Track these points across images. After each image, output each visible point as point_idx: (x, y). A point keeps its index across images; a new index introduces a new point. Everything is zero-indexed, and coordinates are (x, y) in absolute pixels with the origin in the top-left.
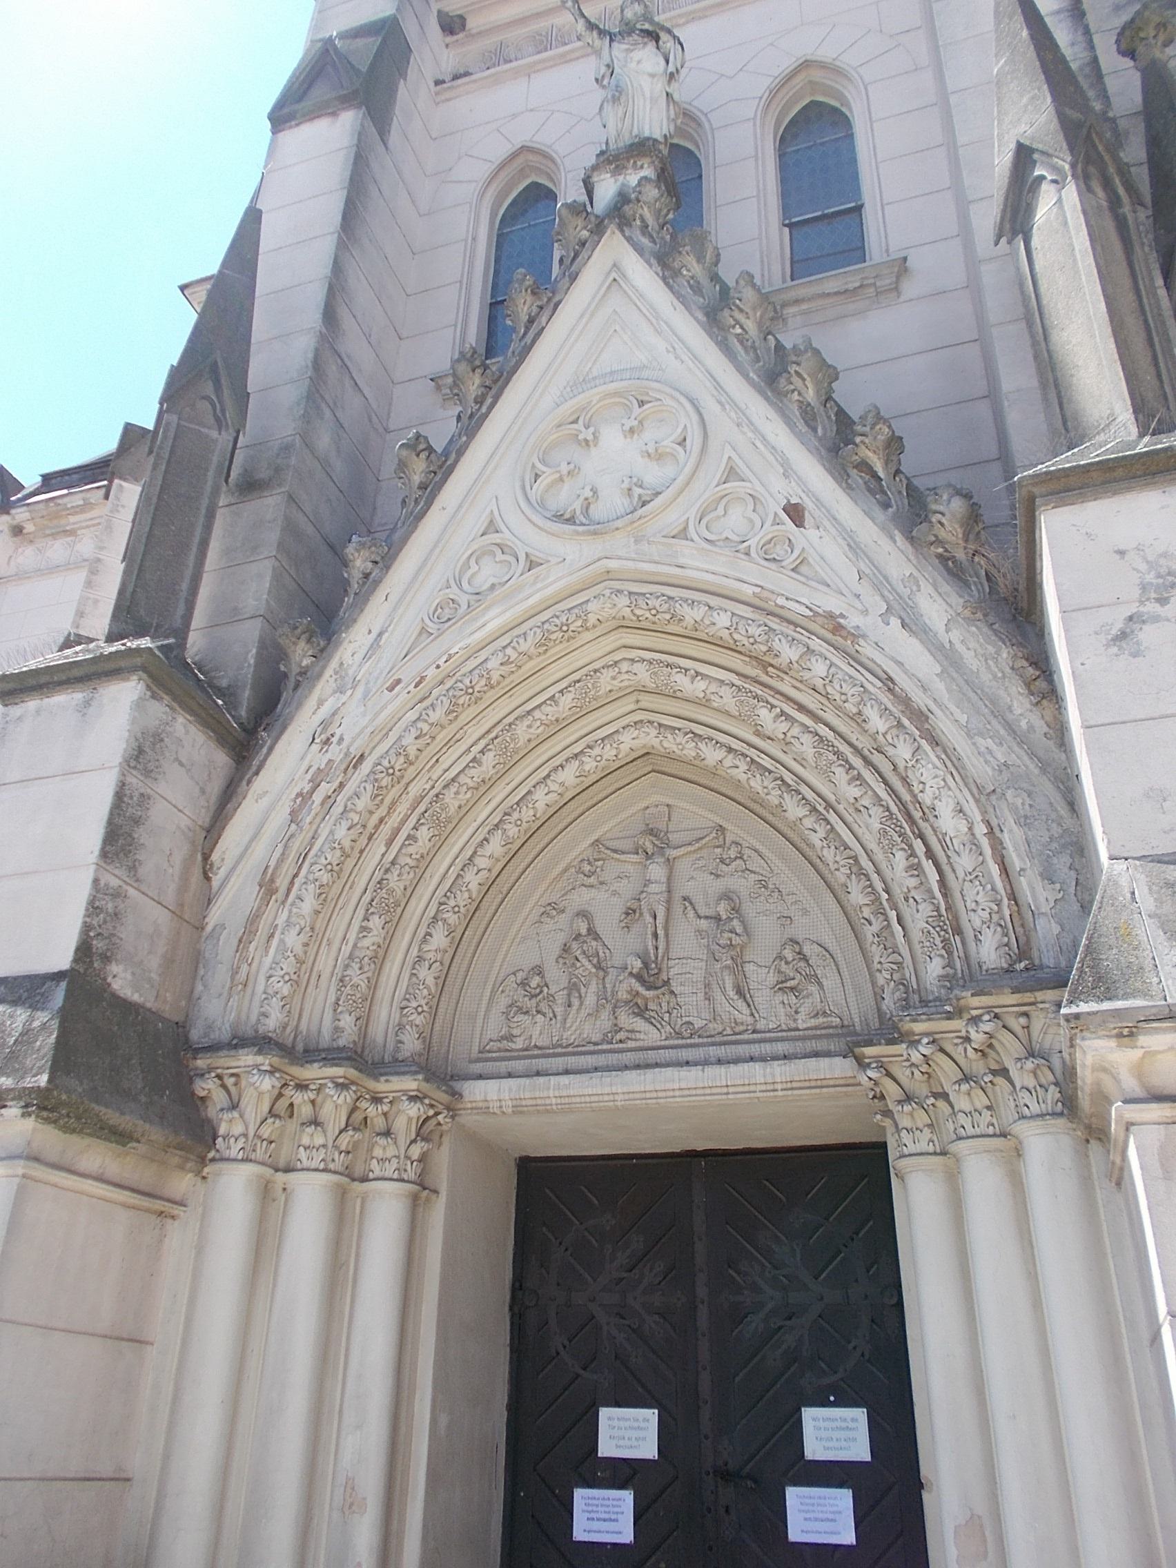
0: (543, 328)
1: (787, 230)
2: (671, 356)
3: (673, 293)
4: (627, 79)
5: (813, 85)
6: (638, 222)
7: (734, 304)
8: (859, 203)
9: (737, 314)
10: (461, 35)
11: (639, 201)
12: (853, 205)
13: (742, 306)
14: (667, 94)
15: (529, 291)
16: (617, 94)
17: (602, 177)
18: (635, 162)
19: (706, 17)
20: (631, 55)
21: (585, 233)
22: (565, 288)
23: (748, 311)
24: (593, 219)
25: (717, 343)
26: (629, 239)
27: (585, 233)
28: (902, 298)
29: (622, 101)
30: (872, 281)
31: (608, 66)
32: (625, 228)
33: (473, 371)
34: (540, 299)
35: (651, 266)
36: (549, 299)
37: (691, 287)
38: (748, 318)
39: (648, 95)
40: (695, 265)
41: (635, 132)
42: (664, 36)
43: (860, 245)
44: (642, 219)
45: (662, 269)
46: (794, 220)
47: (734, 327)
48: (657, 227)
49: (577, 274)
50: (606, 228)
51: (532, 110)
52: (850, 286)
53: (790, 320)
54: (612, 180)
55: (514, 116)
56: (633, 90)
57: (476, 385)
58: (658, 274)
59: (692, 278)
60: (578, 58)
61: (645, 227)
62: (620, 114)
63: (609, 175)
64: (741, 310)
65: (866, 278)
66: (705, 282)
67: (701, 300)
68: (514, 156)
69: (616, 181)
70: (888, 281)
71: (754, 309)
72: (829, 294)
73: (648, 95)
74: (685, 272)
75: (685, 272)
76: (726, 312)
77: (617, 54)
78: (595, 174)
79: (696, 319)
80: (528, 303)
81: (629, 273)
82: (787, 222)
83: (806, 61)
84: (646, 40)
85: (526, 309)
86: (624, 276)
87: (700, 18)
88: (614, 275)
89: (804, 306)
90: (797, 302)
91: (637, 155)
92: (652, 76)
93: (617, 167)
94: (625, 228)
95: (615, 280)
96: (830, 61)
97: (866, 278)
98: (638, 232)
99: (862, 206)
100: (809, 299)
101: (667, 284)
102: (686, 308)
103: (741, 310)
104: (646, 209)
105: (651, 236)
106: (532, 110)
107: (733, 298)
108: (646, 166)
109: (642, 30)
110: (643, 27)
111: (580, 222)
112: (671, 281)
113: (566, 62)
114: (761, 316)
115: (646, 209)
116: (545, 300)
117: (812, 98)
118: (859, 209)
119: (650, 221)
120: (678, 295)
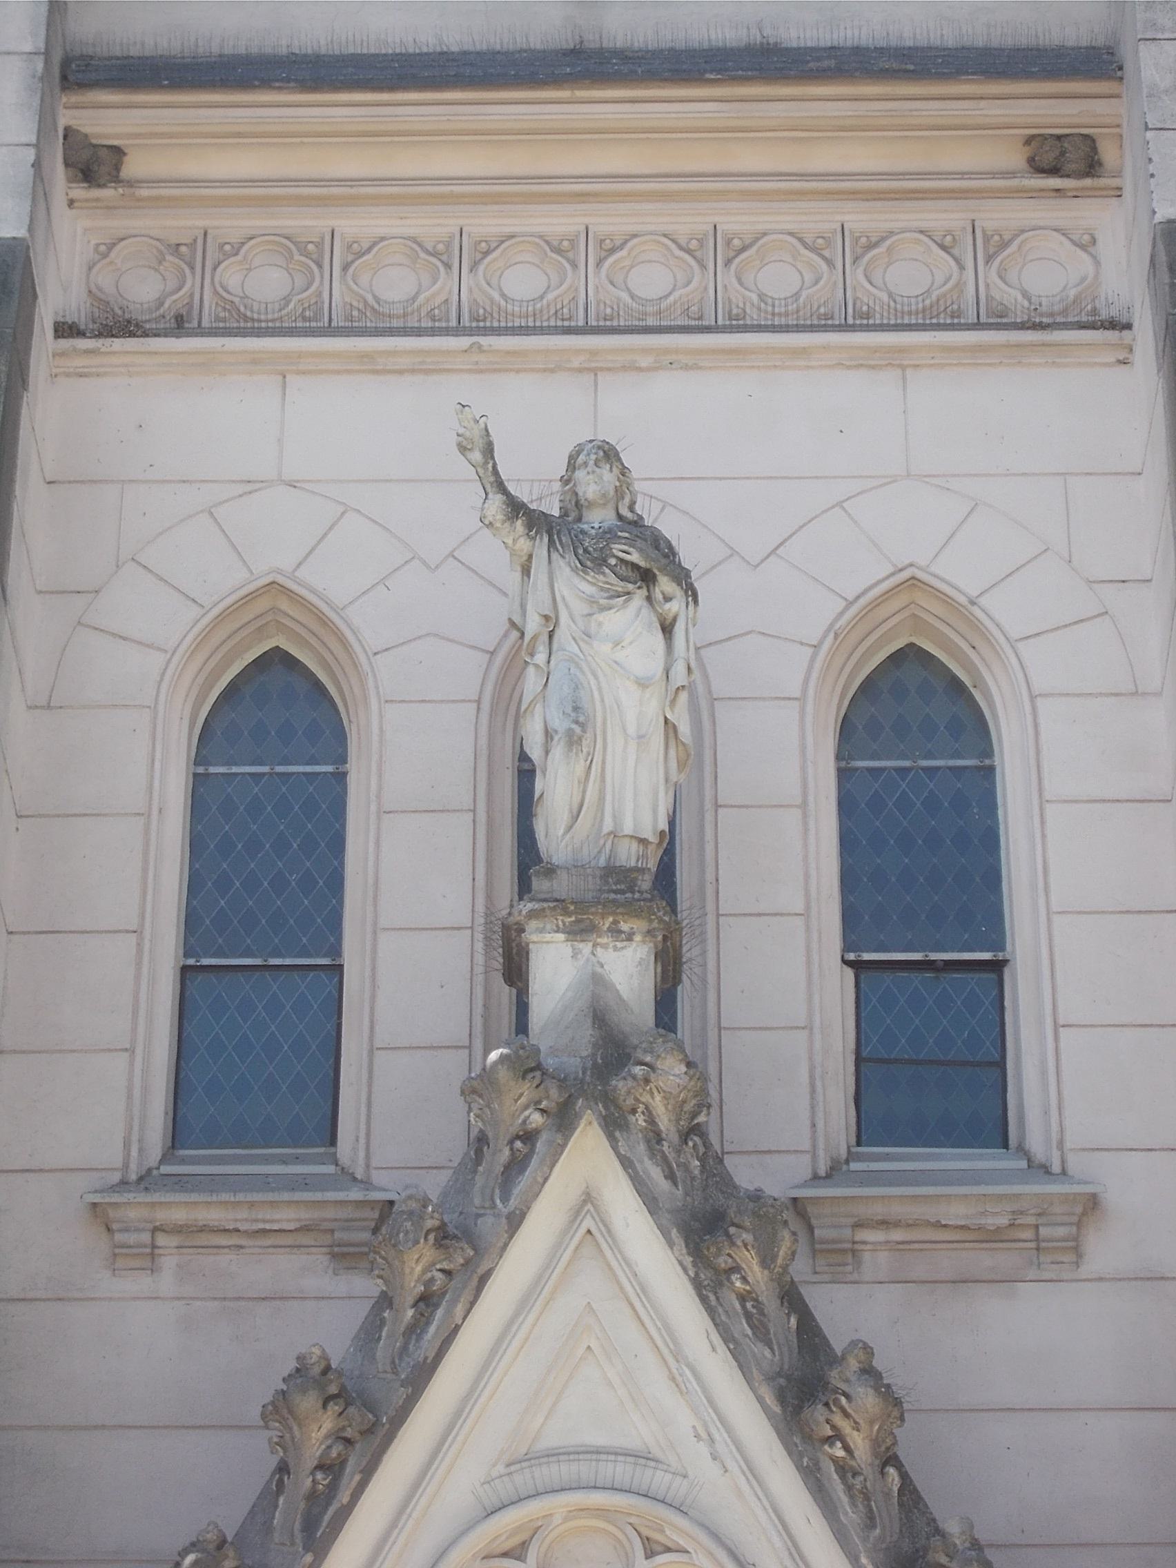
0: (457, 1328)
1: (850, 973)
2: (703, 1449)
3: (716, 1325)
4: (593, 682)
5: (917, 623)
6: (641, 1120)
7: (836, 1402)
8: (1000, 956)
9: (838, 1419)
10: (107, 193)
12: (986, 956)
13: (849, 1410)
14: (666, 720)
15: (431, 1237)
16: (578, 730)
17: (548, 937)
18: (615, 922)
19: (700, 368)
20: (601, 617)
22: (500, 1244)
23: (861, 1422)
24: (554, 1093)
25: (799, 1467)
26: (626, 1163)
27: (537, 1119)
28: (1086, 1270)
29: (584, 742)
30: (1031, 1220)
31: (547, 618)
32: (617, 1134)
33: (325, 1406)
34: (449, 1258)
35: (671, 1244)
36: (467, 1262)
37: (748, 1316)
38: (858, 1430)
39: (632, 730)
40: (756, 1268)
41: (608, 825)
42: (665, 584)
43: (997, 1057)
45: (695, 1264)
46: (866, 956)
47: (829, 1440)
48: (675, 1138)
49: (523, 1216)
50: (578, 1116)
51: (292, 485)
52: (991, 1222)
53: (867, 1257)
54: (567, 949)
55: (251, 485)
56: (604, 712)
57: (324, 1431)
58: (685, 1269)
60: (401, 372)
61: (654, 1137)
62: (580, 768)
63: (561, 937)
64: (846, 1415)
65: (1022, 1213)
67: (767, 1353)
69: (574, 956)
70: (1061, 1231)
73: (632, 730)
74: (738, 1284)
75: (738, 1284)
76: (820, 1413)
77: (566, 593)
78: (533, 925)
79: (760, 1400)
81: (618, 1224)
82: (851, 956)
83: (913, 578)
84: (630, 587)
85: (419, 1269)
86: (609, 1231)
87: (686, 368)
88: (588, 1223)
89: (897, 1235)
90: (885, 1224)
91: (622, 914)
92: (643, 684)
93: (578, 921)
94: (617, 1134)
95: (589, 1232)
96: (962, 600)
97: (1022, 1213)
98: (642, 1147)
99: (1005, 962)
100: (909, 1225)
101: (704, 1300)
102: (741, 1367)
103: (846, 1415)
104: (658, 1098)
106: (292, 485)
107: (836, 1390)
108: (638, 938)
110: (628, 557)
111: (527, 1090)
112: (712, 1297)
113: (377, 372)
114: (879, 1430)
115: (658, 1098)
117: (914, 640)
118: (997, 967)
119: (665, 1123)
120: (727, 1337)
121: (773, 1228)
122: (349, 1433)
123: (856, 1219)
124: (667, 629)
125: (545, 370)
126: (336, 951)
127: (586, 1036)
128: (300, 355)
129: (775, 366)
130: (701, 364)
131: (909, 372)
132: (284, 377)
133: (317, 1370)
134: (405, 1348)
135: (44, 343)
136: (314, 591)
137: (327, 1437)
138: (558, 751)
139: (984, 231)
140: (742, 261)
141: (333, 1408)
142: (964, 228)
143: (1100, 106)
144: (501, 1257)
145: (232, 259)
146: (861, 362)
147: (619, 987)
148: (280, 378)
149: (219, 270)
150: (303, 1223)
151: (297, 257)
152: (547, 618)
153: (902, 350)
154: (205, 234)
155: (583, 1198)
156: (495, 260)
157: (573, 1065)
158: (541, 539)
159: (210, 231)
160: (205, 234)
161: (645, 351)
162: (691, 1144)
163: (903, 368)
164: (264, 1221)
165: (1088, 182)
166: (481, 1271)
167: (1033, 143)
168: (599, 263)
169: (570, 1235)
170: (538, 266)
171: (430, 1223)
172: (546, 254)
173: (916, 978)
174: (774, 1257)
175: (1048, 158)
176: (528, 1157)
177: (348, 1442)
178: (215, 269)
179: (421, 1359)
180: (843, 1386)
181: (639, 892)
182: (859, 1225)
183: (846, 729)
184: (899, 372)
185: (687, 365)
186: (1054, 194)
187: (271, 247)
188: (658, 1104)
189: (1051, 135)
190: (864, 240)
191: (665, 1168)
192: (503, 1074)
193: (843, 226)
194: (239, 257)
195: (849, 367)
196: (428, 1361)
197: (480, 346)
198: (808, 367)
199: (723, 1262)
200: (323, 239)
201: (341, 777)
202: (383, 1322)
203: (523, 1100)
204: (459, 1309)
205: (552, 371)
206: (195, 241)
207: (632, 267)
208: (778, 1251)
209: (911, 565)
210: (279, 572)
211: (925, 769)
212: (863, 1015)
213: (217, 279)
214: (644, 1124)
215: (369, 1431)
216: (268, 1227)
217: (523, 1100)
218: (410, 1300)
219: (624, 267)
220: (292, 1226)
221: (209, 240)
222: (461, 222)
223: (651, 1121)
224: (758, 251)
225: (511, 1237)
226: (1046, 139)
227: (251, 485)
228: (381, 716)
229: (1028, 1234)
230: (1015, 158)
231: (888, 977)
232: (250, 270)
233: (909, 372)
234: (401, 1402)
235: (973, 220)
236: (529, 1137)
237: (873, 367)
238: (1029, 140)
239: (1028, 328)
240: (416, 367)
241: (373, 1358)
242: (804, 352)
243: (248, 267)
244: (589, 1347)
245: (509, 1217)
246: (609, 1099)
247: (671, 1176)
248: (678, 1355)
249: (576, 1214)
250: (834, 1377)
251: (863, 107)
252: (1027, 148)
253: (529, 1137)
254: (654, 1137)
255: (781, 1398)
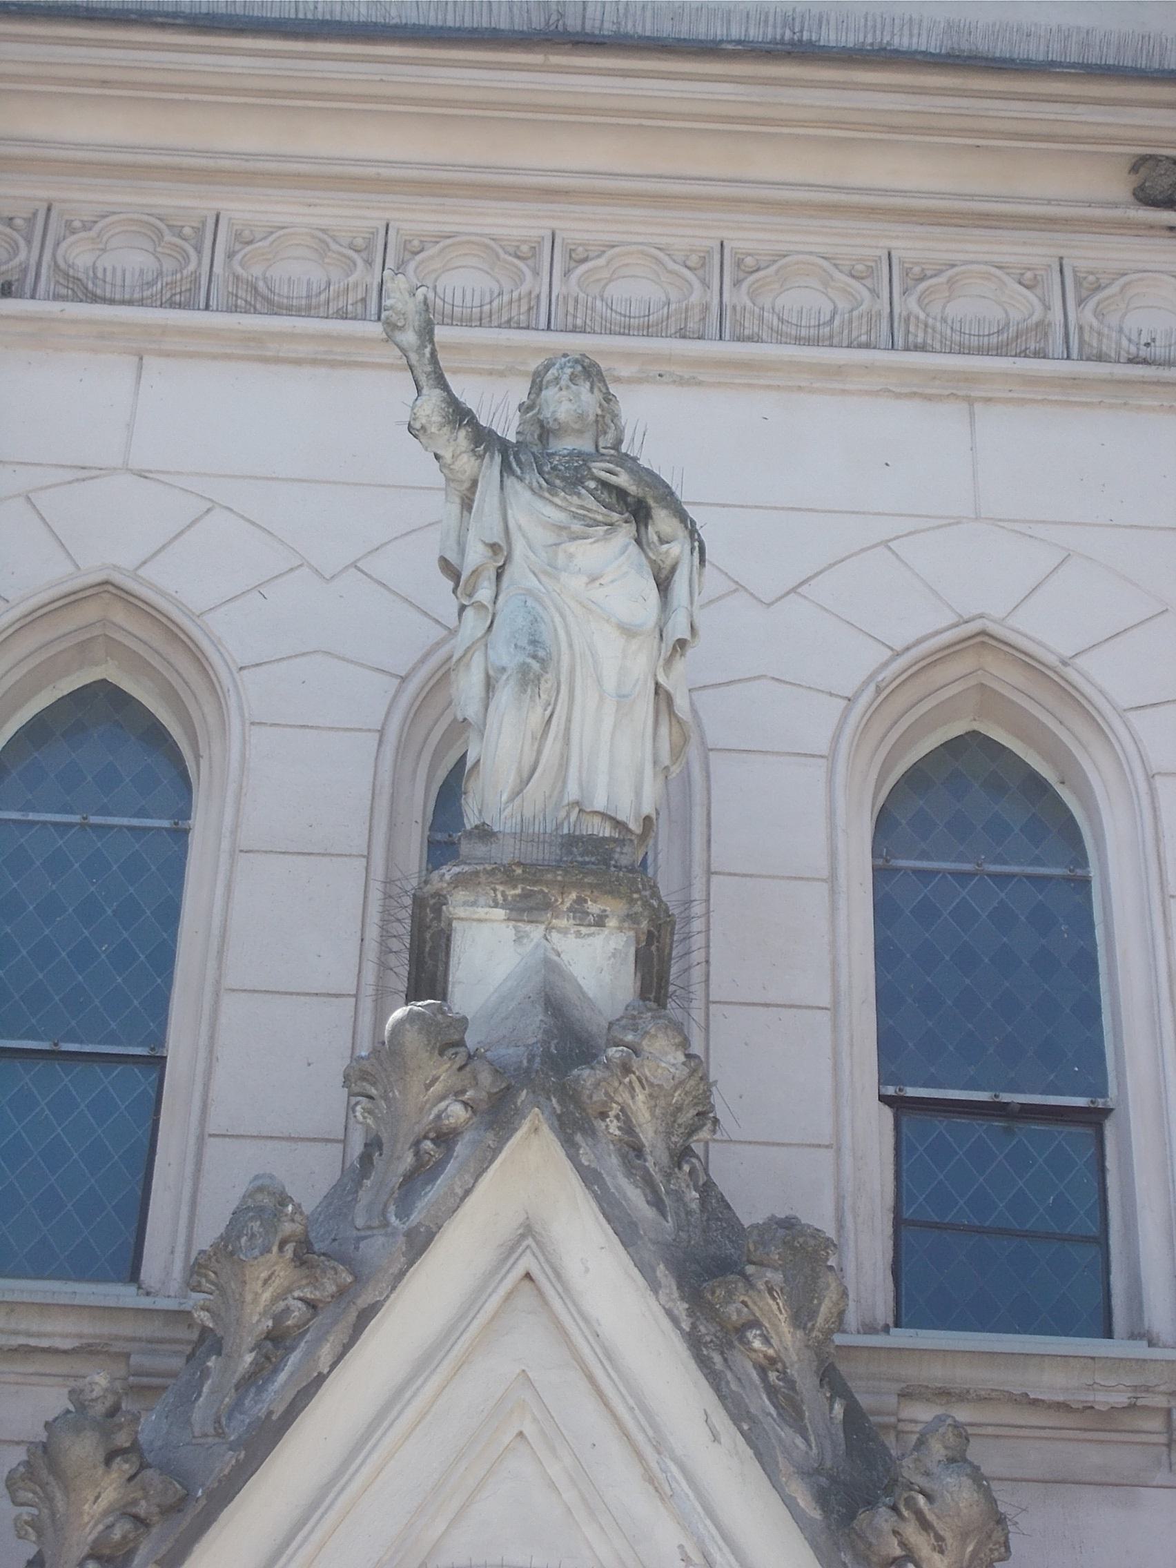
0: (321, 1379)
1: (888, 1113)
3: (722, 1397)
4: (558, 619)
5: (987, 698)
6: (614, 1127)
7: (910, 1503)
8: (1100, 1103)
9: (912, 1532)
11: (626, 1069)
12: (1081, 1102)
13: (930, 1517)
14: (658, 686)
15: (289, 1248)
16: (536, 666)
17: (481, 912)
18: (580, 901)
19: (700, 383)
20: (572, 547)
21: (457, 1113)
22: (394, 1270)
23: (947, 1535)
24: (485, 1077)
26: (590, 1177)
27: (457, 1113)
29: (543, 686)
30: (1160, 1401)
31: (494, 548)
32: (579, 1138)
33: (108, 1461)
34: (314, 1282)
35: (654, 1286)
36: (342, 1292)
37: (771, 1391)
38: (941, 1552)
39: (610, 685)
40: (785, 1327)
41: (573, 792)
42: (663, 521)
43: (1094, 1230)
44: (625, 1118)
45: (691, 1313)
46: (911, 1092)
48: (665, 1159)
49: (430, 1237)
50: (520, 1114)
51: (142, 474)
52: (1103, 1400)
54: (508, 931)
56: (573, 656)
57: (103, 1503)
58: (675, 1321)
59: (772, 1361)
60: (298, 362)
61: (632, 1150)
62: (536, 718)
63: (500, 913)
64: (925, 1525)
65: (1147, 1389)
66: (807, 1383)
67: (799, 1441)
68: (73, 600)
69: (518, 940)
71: (964, 1536)
72: (1035, 1403)
73: (610, 685)
74: (757, 1344)
75: (757, 1344)
76: (883, 1519)
77: (523, 521)
78: (460, 895)
79: (789, 1503)
80: (276, 1283)
81: (572, 1268)
82: (890, 1090)
83: (983, 633)
84: (615, 516)
85: (267, 1295)
86: (558, 1275)
87: (681, 382)
88: (527, 1262)
91: (592, 887)
92: (628, 631)
93: (526, 896)
94: (579, 1138)
95: (528, 1276)
96: (1052, 660)
97: (1147, 1389)
98: (614, 1161)
99: (1107, 1112)
101: (704, 1363)
102: (759, 1455)
103: (925, 1525)
104: (641, 1097)
105: (648, 1183)
106: (142, 474)
107: (909, 1486)
108: (612, 923)
109: (605, 484)
110: (613, 479)
111: (444, 1072)
112: (717, 1358)
113: (264, 360)
114: (975, 1554)
115: (641, 1097)
116: (331, 1288)
117: (976, 726)
118: (1095, 1118)
119: (648, 1133)
120: (738, 1413)
121: (813, 1269)
122: (142, 1509)
123: (904, 1385)
124: (663, 584)
125: (491, 373)
126: (159, 1038)
127: (535, 1024)
128: (165, 330)
129: (800, 388)
130: (701, 378)
131: (978, 407)
132: (141, 359)
133: (100, 1409)
134: (237, 1406)
136: (163, 594)
137: (106, 1513)
138: (505, 695)
139: (1075, 272)
140: (757, 281)
141: (123, 1467)
142: (1049, 266)
144: (394, 1288)
145: (83, 234)
146: (915, 389)
147: (581, 982)
148: (136, 359)
149: (64, 245)
150: (85, 1341)
151: (168, 237)
152: (494, 548)
153: (971, 378)
154: (49, 209)
155: (520, 1231)
156: (432, 258)
157: (511, 1054)
158: (492, 458)
159: (54, 204)
160: (49, 209)
162: (686, 1168)
163: (970, 401)
164: (29, 1334)
166: (364, 1301)
167: (1142, 169)
168: (567, 273)
169: (499, 1277)
170: (488, 273)
171: (287, 1228)
172: (498, 257)
173: (979, 1128)
174: (813, 1315)
176: (440, 1166)
177: (141, 1522)
178: (58, 244)
179: (262, 1414)
180: (920, 1480)
181: (615, 866)
182: (906, 1395)
183: (884, 823)
184: (965, 405)
185: (681, 378)
186: (1168, 233)
187: (134, 228)
188: (641, 1108)
189: (1167, 158)
190: (917, 270)
191: (648, 1191)
192: (413, 1039)
193: (889, 254)
194: (92, 234)
195: (898, 396)
196: (274, 1417)
198: (844, 392)
199: (733, 1312)
200: (204, 223)
201: (181, 835)
202: (205, 1373)
203: (437, 1088)
204: (326, 1353)
205: (501, 374)
206: (35, 214)
207: (610, 280)
208: (820, 1304)
209: (981, 616)
210: (115, 567)
211: (994, 876)
212: (905, 1167)
213: (60, 252)
214: (617, 1132)
215: (172, 1509)
216: (33, 1342)
217: (437, 1088)
218: (250, 1341)
219: (598, 280)
220: (67, 1344)
221: (54, 214)
222: (388, 215)
223: (628, 1128)
224: (777, 272)
225: (411, 1263)
226: (1161, 161)
227: (86, 472)
228: (244, 742)
229: (1156, 1424)
230: (1118, 187)
231: (940, 1125)
232: (104, 250)
233: (978, 407)
234: (226, 1472)
235: (1061, 258)
236: (445, 1138)
237: (928, 398)
238: (1139, 163)
239: (1138, 363)
240: (319, 357)
241: (188, 1422)
242: (838, 371)
243: (101, 246)
244: (521, 1434)
245: (409, 1234)
246: (569, 1093)
247: (657, 1203)
248: (659, 1445)
249: (510, 1250)
250: (908, 1470)
251: (922, 103)
252: (1133, 177)
253: (445, 1138)
254: (632, 1150)
255: (822, 1498)
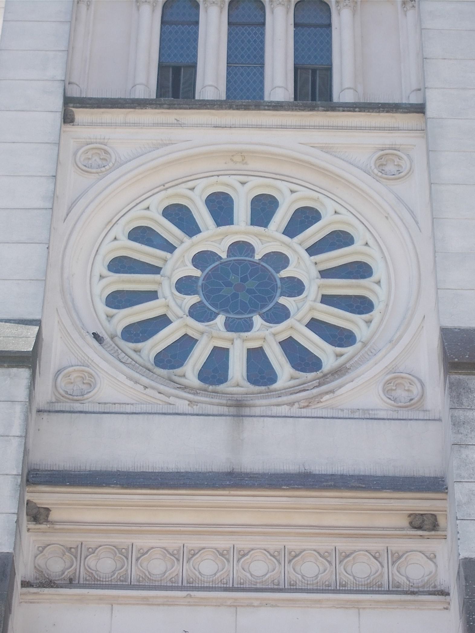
10: (43, 526)
60: (159, 605)
87: (272, 606)
125: (216, 606)
128: (119, 597)
129: (308, 607)
130: (278, 605)
131: (361, 610)
132: (112, 606)
135: (18, 589)
139: (391, 551)
140: (296, 561)
142: (384, 550)
143: (438, 503)
145: (92, 555)
146: (342, 606)
148: (110, 606)
149: (87, 559)
151: (118, 555)
153: (358, 602)
154: (82, 544)
156: (197, 558)
159: (83, 543)
160: (82, 544)
161: (257, 599)
163: (359, 609)
165: (433, 533)
167: (412, 516)
168: (239, 560)
170: (214, 561)
172: (217, 557)
175: (417, 523)
178: (85, 558)
184: (357, 610)
185: (273, 605)
186: (420, 537)
187: (108, 550)
189: (419, 514)
190: (344, 554)
193: (335, 547)
194: (95, 554)
195: (337, 608)
197: (191, 596)
198: (321, 607)
200: (128, 547)
205: (219, 606)
206: (78, 546)
207: (251, 562)
213: (86, 563)
219: (248, 563)
221: (83, 545)
222: (183, 542)
224: (301, 557)
226: (417, 515)
230: (404, 522)
232: (99, 559)
233: (361, 610)
235: (387, 547)
237: (347, 608)
238: (410, 515)
239: (409, 594)
240: (165, 603)
242: (319, 601)
243: (98, 558)
251: (344, 501)
252: (409, 518)
